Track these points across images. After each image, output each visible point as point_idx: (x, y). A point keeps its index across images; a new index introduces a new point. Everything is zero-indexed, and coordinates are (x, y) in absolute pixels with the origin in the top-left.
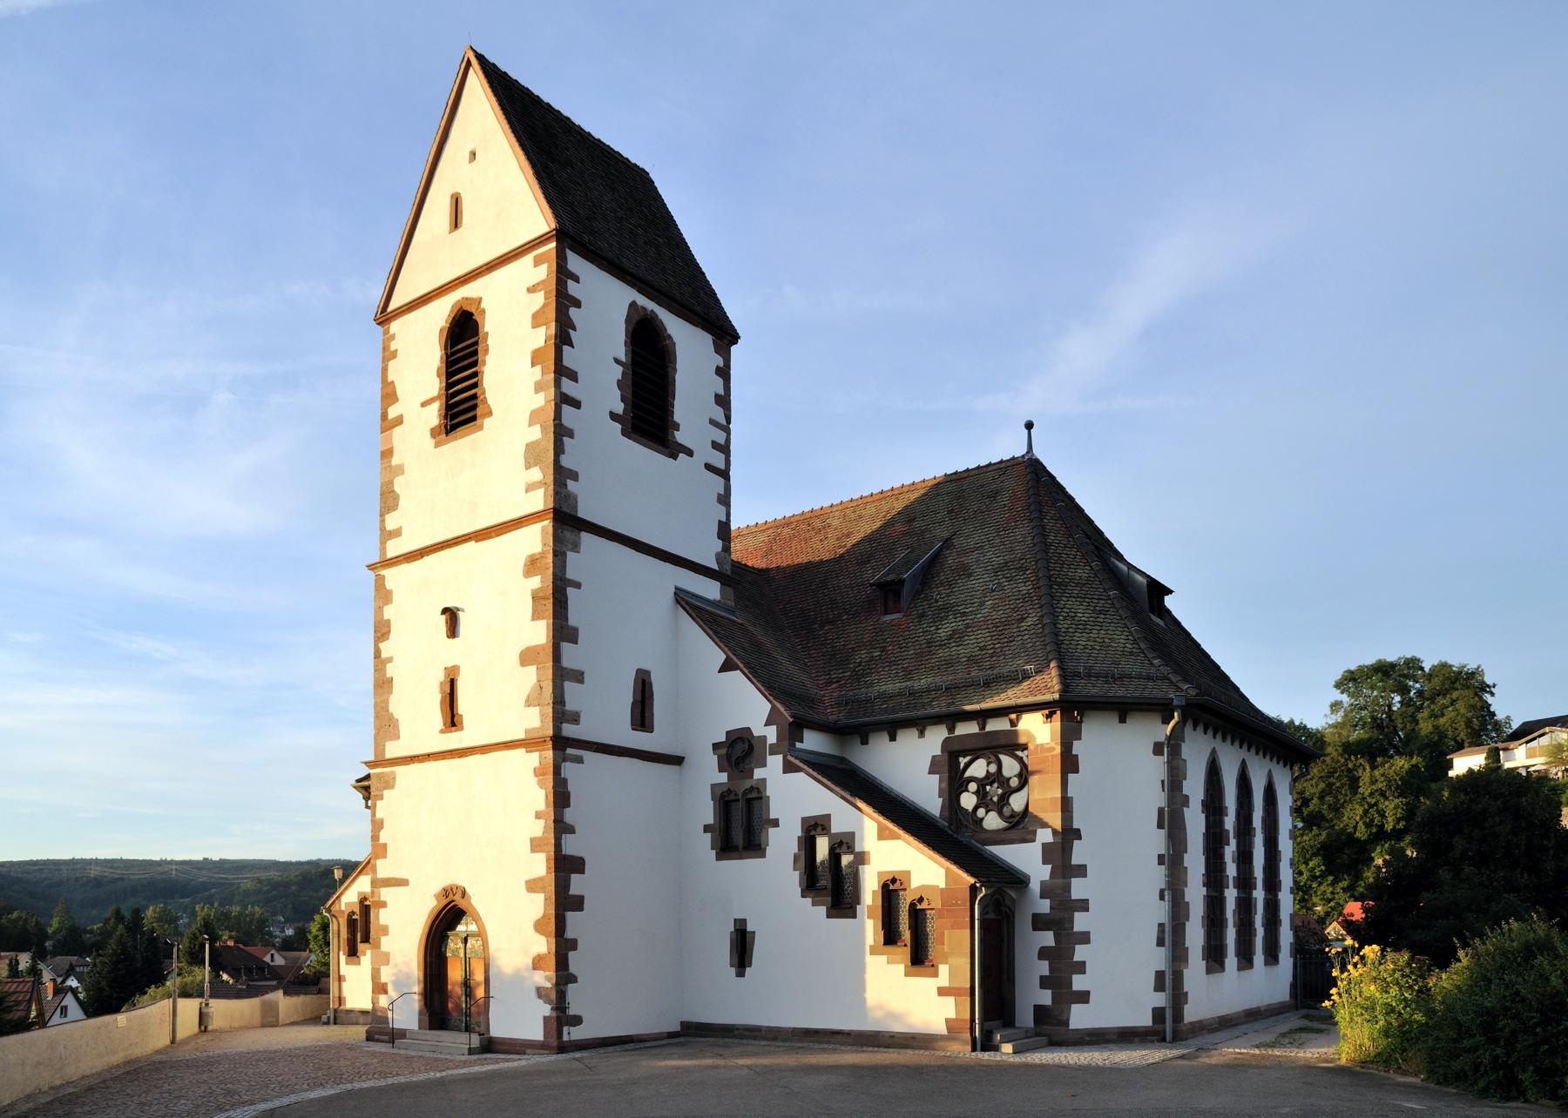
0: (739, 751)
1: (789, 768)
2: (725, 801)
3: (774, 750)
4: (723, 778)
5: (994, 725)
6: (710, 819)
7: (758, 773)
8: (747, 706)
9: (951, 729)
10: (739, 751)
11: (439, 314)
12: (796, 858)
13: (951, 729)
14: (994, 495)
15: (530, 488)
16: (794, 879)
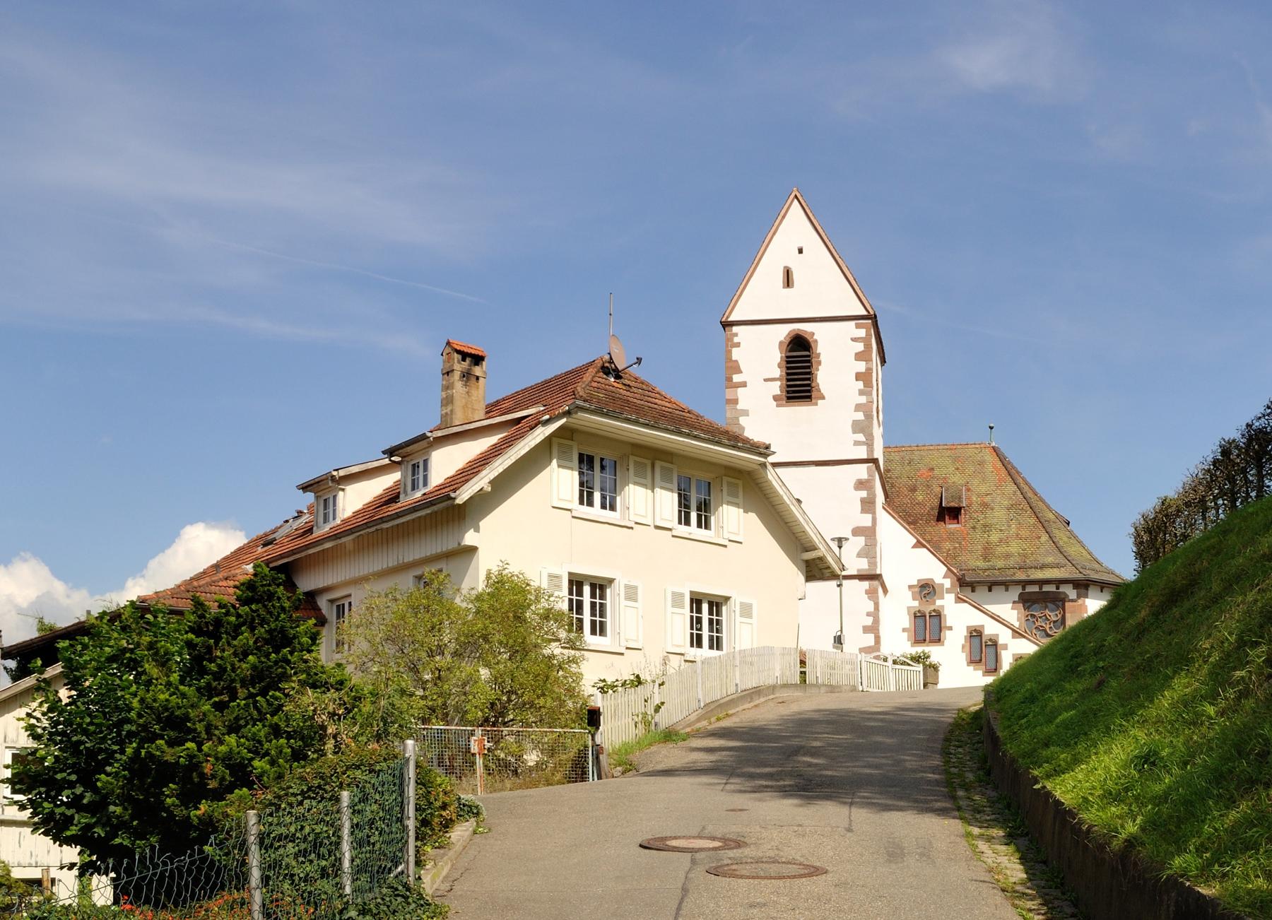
0: (926, 589)
1: (959, 600)
2: (918, 616)
3: (949, 591)
4: (916, 604)
5: (1046, 588)
6: (907, 625)
7: (939, 603)
8: (935, 570)
9: (1024, 588)
10: (926, 589)
11: (783, 332)
12: (963, 647)
13: (1024, 588)
14: (981, 463)
15: (857, 443)
16: (962, 658)
